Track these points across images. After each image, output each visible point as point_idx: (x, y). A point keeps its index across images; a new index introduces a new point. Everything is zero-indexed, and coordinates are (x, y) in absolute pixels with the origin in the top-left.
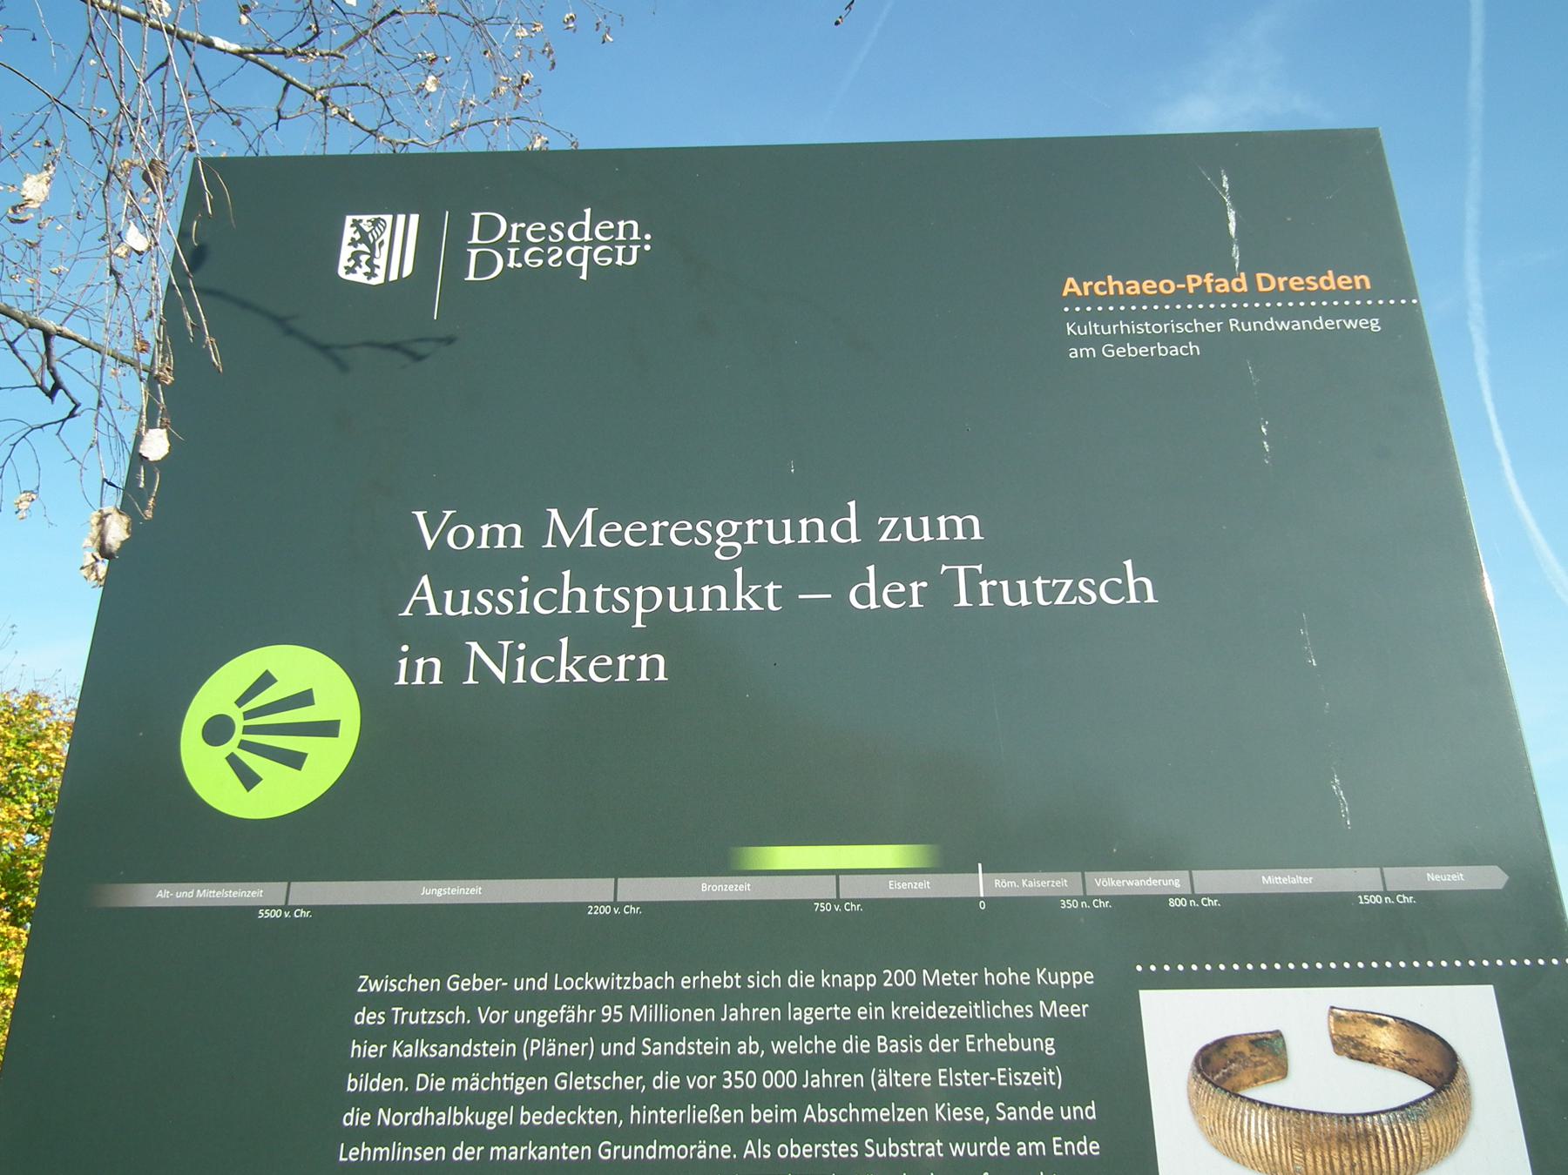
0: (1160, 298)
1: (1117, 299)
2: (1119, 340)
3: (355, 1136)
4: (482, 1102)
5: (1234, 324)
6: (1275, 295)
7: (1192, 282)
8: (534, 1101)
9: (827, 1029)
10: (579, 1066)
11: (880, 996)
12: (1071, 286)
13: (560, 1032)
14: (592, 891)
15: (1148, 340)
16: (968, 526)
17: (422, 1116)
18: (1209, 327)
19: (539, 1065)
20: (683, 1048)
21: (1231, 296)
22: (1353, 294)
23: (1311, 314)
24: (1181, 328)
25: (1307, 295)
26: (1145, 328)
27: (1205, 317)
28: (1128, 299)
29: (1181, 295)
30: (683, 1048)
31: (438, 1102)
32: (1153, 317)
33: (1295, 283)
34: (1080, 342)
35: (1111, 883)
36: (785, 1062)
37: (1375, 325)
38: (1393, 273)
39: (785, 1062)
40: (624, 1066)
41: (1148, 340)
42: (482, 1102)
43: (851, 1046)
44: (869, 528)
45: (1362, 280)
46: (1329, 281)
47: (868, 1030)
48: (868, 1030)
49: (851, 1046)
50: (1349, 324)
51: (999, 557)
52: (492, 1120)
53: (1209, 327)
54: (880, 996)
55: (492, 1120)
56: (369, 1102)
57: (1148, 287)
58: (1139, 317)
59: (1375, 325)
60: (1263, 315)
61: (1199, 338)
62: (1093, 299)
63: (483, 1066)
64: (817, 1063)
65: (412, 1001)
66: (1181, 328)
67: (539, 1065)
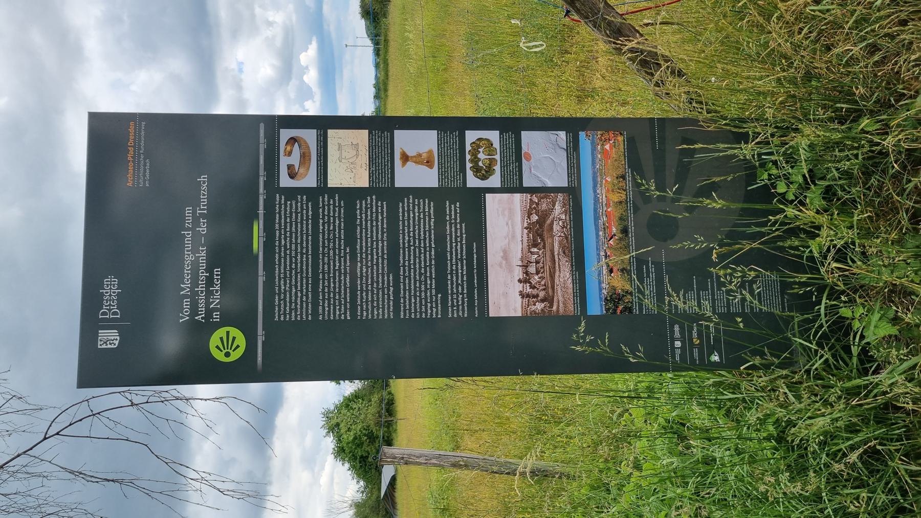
0: (134, 166)
2: (144, 176)
3: (302, 317)
4: (296, 297)
6: (135, 142)
7: (130, 158)
8: (296, 288)
9: (285, 239)
10: (291, 281)
11: (280, 230)
13: (285, 285)
14: (261, 280)
15: (145, 170)
16: (188, 210)
17: (299, 306)
18: (142, 157)
19: (290, 288)
20: (288, 263)
22: (135, 124)
24: (142, 163)
25: (135, 136)
26: (142, 171)
30: (288, 263)
31: (296, 304)
32: (139, 169)
33: (131, 137)
35: (261, 190)
36: (291, 246)
39: (291, 246)
40: (291, 273)
41: (145, 170)
42: (296, 297)
43: (288, 235)
44: (188, 229)
46: (132, 130)
47: (286, 232)
48: (286, 232)
49: (288, 235)
51: (196, 204)
52: (299, 295)
53: (142, 157)
54: (280, 230)
55: (299, 295)
56: (296, 316)
61: (145, 159)
63: (291, 296)
64: (291, 241)
65: (279, 310)
67: (290, 288)
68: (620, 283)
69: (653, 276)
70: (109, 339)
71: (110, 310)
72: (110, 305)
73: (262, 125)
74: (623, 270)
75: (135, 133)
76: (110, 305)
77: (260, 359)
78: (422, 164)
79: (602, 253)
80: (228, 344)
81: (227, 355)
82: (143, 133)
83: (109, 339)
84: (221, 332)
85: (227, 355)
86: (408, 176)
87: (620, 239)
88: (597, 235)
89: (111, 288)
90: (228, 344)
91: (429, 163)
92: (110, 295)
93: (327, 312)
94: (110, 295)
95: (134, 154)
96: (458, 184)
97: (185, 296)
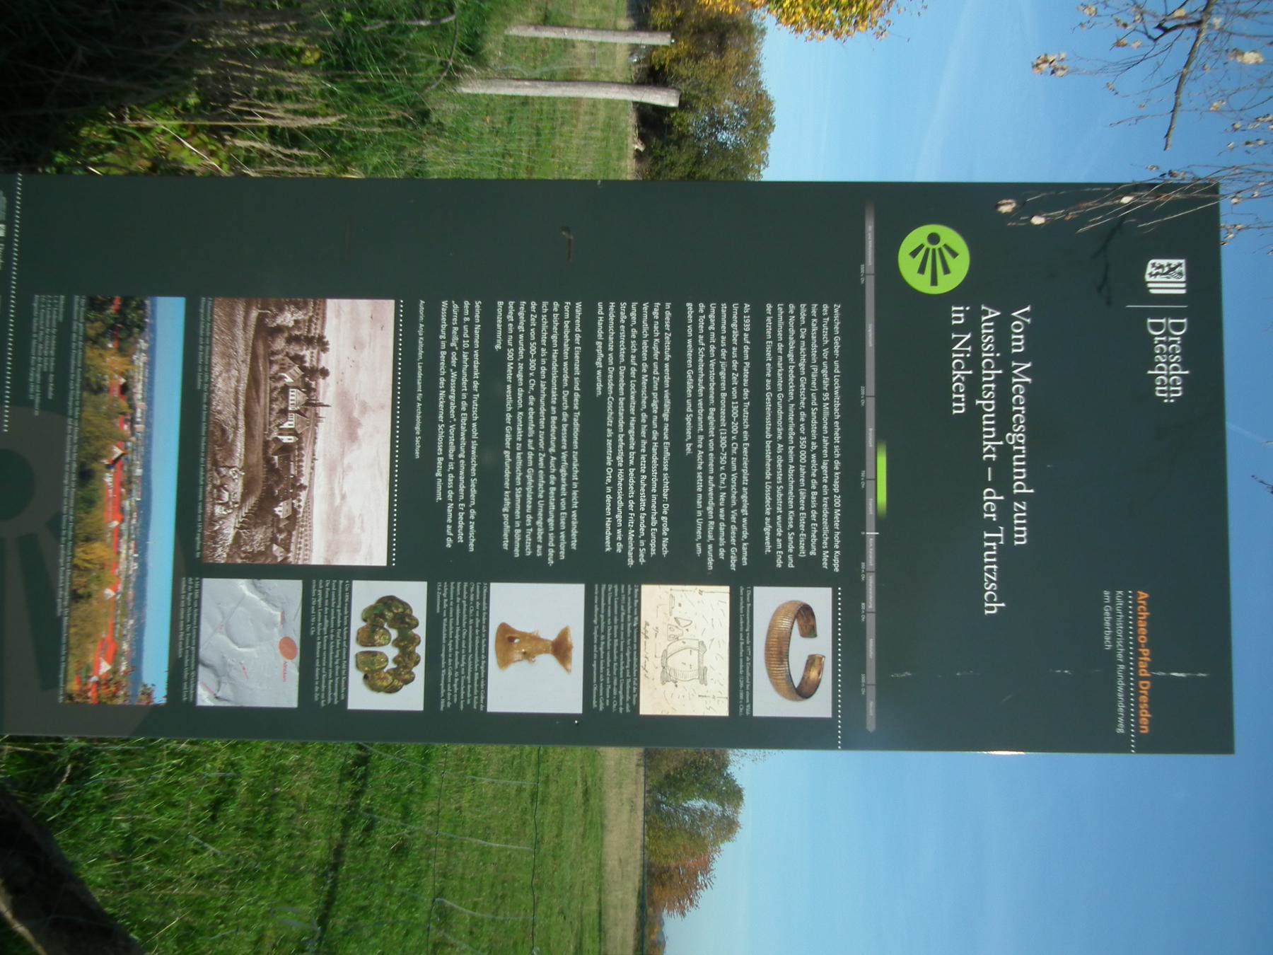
0: (1136, 635)
1: (1136, 616)
2: (1114, 614)
3: (786, 309)
4: (797, 352)
5: (1122, 667)
6: (1137, 688)
7: (1145, 651)
8: (797, 370)
9: (820, 473)
10: (808, 385)
11: (831, 494)
12: (1143, 595)
13: (820, 378)
14: (870, 388)
15: (1113, 626)
17: (792, 331)
18: (1120, 656)
19: (809, 371)
20: (814, 422)
21: (1137, 668)
22: (1137, 724)
23: (1127, 702)
24: (1119, 643)
25: (1137, 703)
26: (1120, 626)
27: (1126, 655)
28: (1135, 620)
29: (1137, 645)
30: (814, 422)
31: (797, 336)
33: (1144, 699)
34: (1113, 596)
36: (809, 459)
37: (1120, 730)
38: (1148, 745)
39: (809, 459)
40: (808, 402)
41: (1113, 626)
42: (797, 352)
43: (814, 483)
45: (1145, 730)
46: (1145, 716)
47: (819, 489)
48: (819, 489)
49: (814, 483)
50: (1121, 720)
51: (1007, 553)
52: (791, 356)
53: (1120, 656)
54: (831, 494)
55: (791, 356)
57: (1143, 631)
58: (1126, 624)
59: (1120, 730)
60: (1127, 680)
61: (1114, 651)
62: (1136, 604)
63: (808, 352)
64: (808, 470)
65: (831, 324)
66: (1119, 643)
67: (809, 371)
68: (109, 363)
69: (34, 376)
70: (1165, 277)
71: (1167, 334)
72: (1168, 344)
73: (871, 726)
74: (99, 389)
75: (1137, 708)
76: (1168, 344)
77: (870, 228)
78: (524, 636)
79: (139, 427)
80: (933, 261)
81: (934, 238)
82: (1121, 708)
83: (1165, 277)
84: (947, 284)
85: (934, 238)
86: (550, 608)
87: (96, 457)
88: (146, 467)
89: (1168, 377)
90: (933, 261)
91: (508, 636)
92: (1168, 363)
93: (733, 319)
94: (1168, 363)
95: (1136, 661)
96: (445, 589)
97: (1021, 358)
